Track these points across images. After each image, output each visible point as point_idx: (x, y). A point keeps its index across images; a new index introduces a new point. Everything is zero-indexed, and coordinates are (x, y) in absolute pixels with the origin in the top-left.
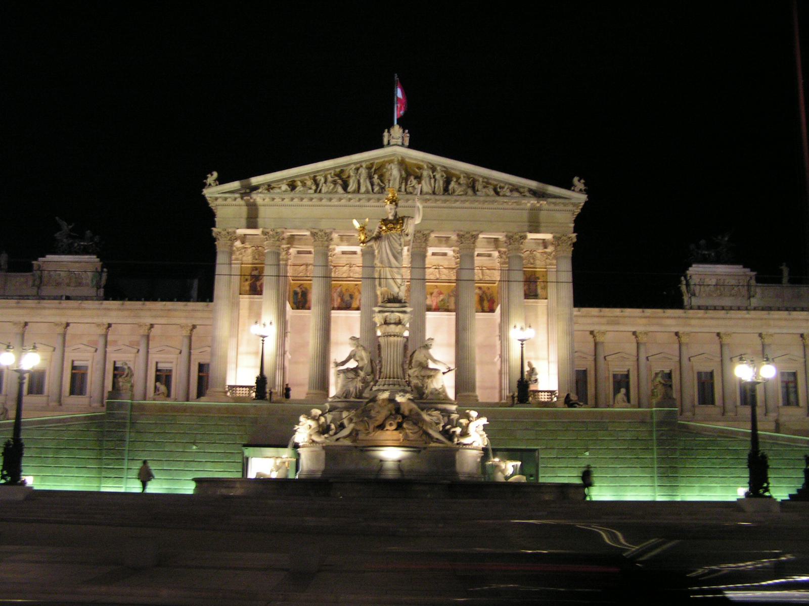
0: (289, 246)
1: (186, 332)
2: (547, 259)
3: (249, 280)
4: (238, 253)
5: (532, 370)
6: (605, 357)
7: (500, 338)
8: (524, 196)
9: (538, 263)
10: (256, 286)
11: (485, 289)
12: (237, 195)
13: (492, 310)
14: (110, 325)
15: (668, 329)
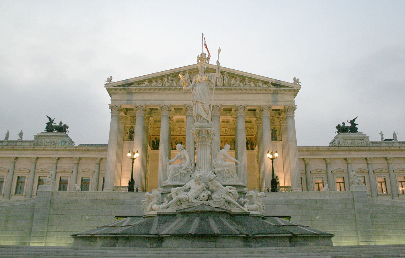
0: (149, 115)
1: (97, 162)
2: (280, 120)
3: (129, 133)
4: (123, 119)
5: (277, 177)
6: (310, 172)
7: (258, 162)
8: (270, 86)
9: (276, 122)
10: (132, 136)
11: (248, 138)
12: (122, 88)
13: (252, 149)
14: (59, 158)
15: (342, 157)
